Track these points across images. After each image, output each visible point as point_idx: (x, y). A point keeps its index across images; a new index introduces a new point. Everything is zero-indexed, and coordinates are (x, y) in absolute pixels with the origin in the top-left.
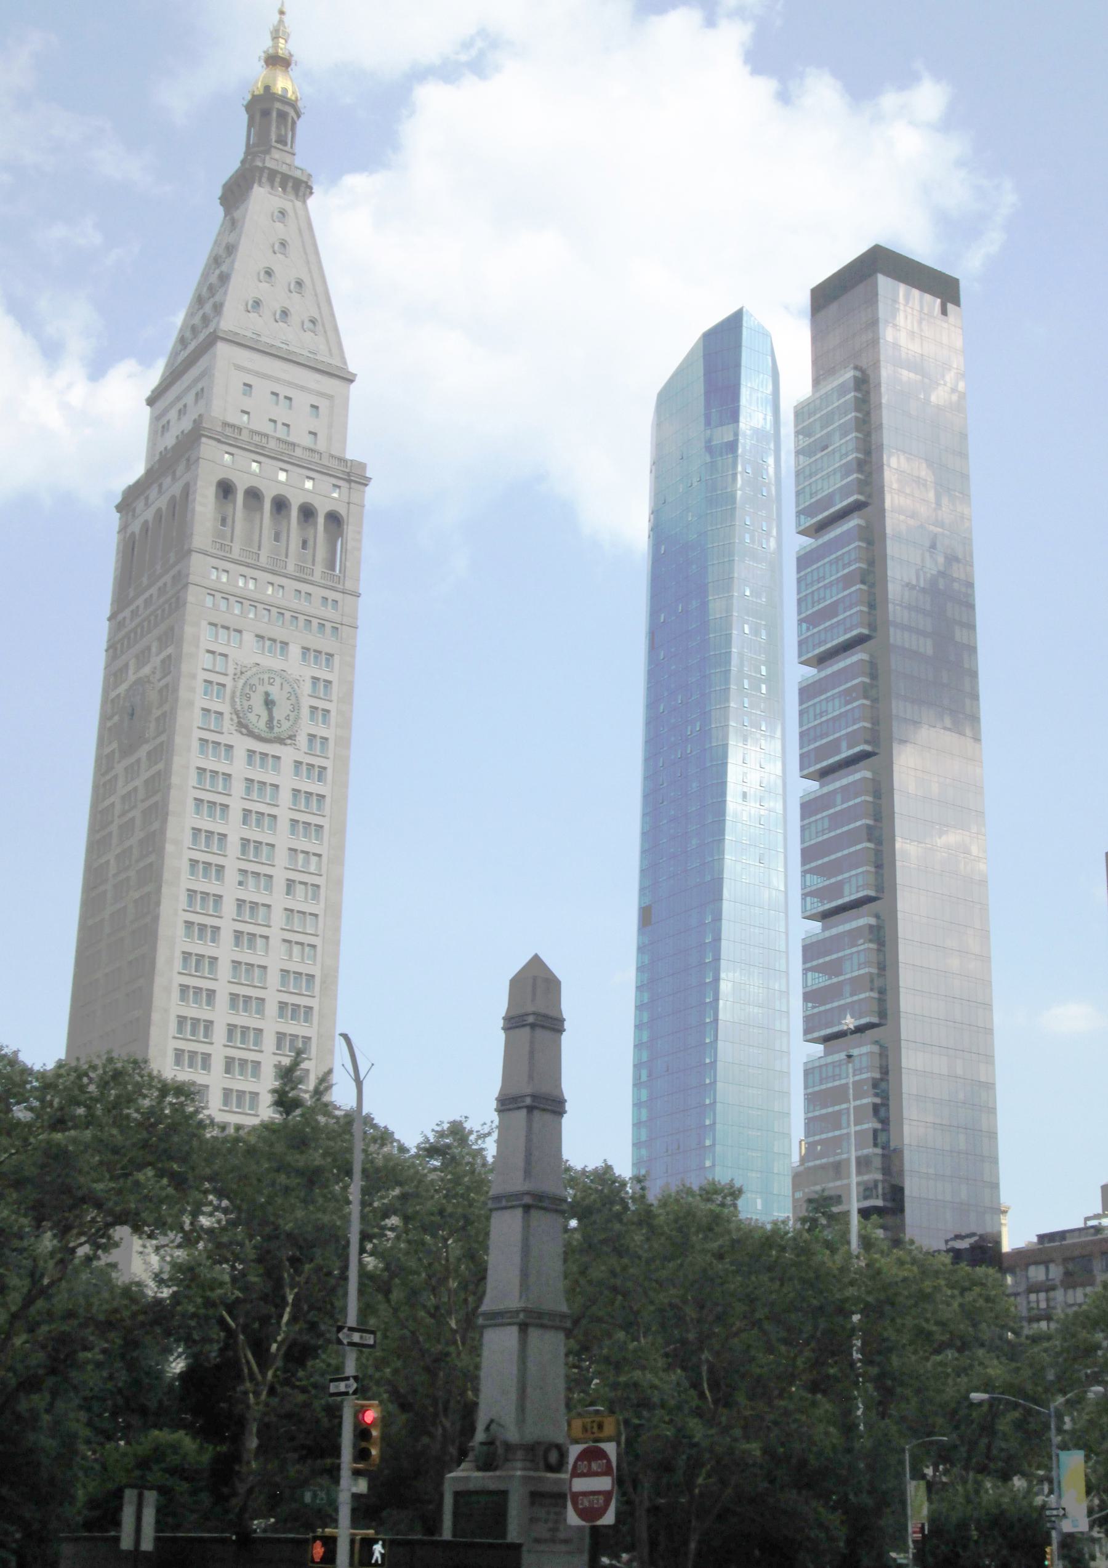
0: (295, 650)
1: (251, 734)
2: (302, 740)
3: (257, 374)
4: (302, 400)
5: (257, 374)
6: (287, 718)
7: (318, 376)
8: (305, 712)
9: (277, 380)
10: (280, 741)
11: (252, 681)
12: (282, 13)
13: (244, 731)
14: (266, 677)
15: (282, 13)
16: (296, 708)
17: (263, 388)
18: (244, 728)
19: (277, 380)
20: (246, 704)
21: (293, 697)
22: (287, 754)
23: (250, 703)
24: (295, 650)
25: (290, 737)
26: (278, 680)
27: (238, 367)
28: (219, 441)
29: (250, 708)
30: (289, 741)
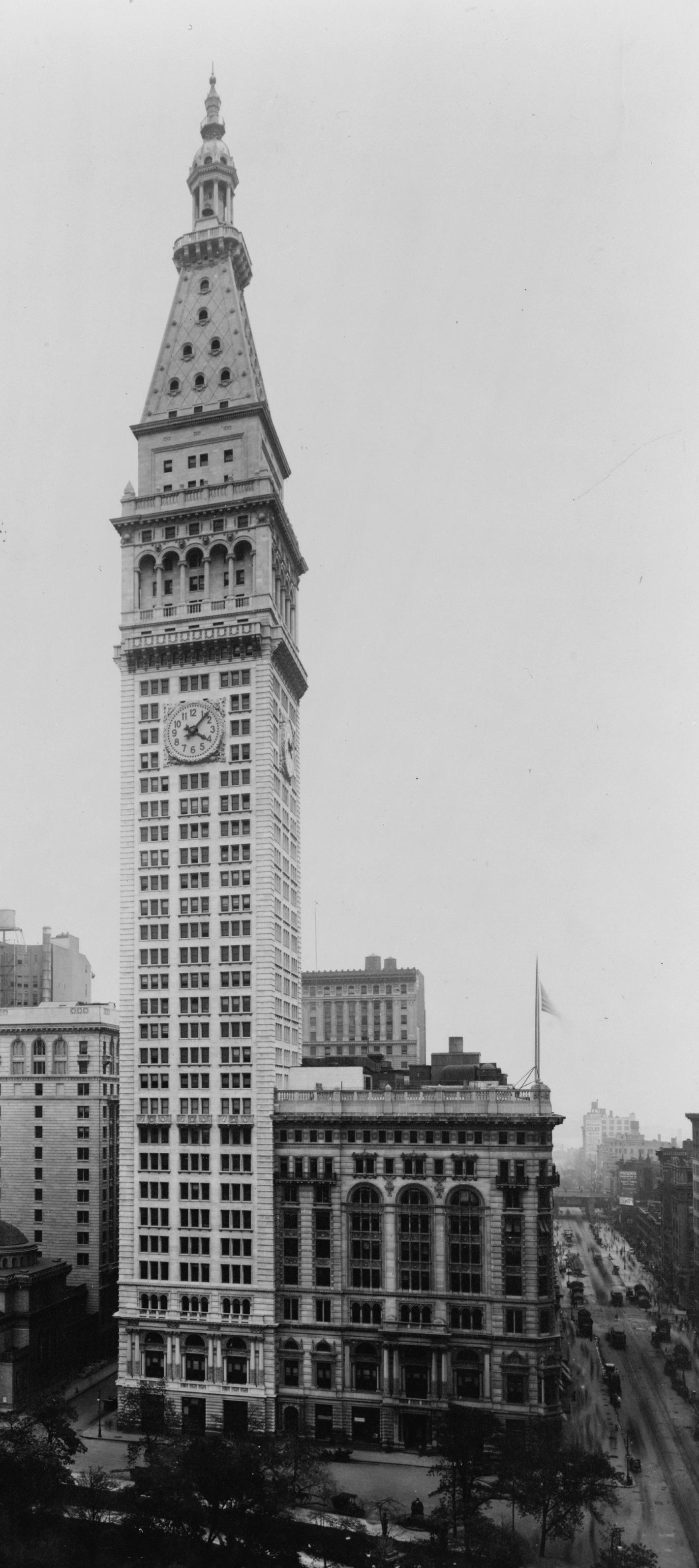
0: (214, 681)
1: (179, 763)
4: (216, 453)
10: (207, 760)
13: (175, 761)
22: (214, 770)
24: (214, 681)
25: (212, 755)
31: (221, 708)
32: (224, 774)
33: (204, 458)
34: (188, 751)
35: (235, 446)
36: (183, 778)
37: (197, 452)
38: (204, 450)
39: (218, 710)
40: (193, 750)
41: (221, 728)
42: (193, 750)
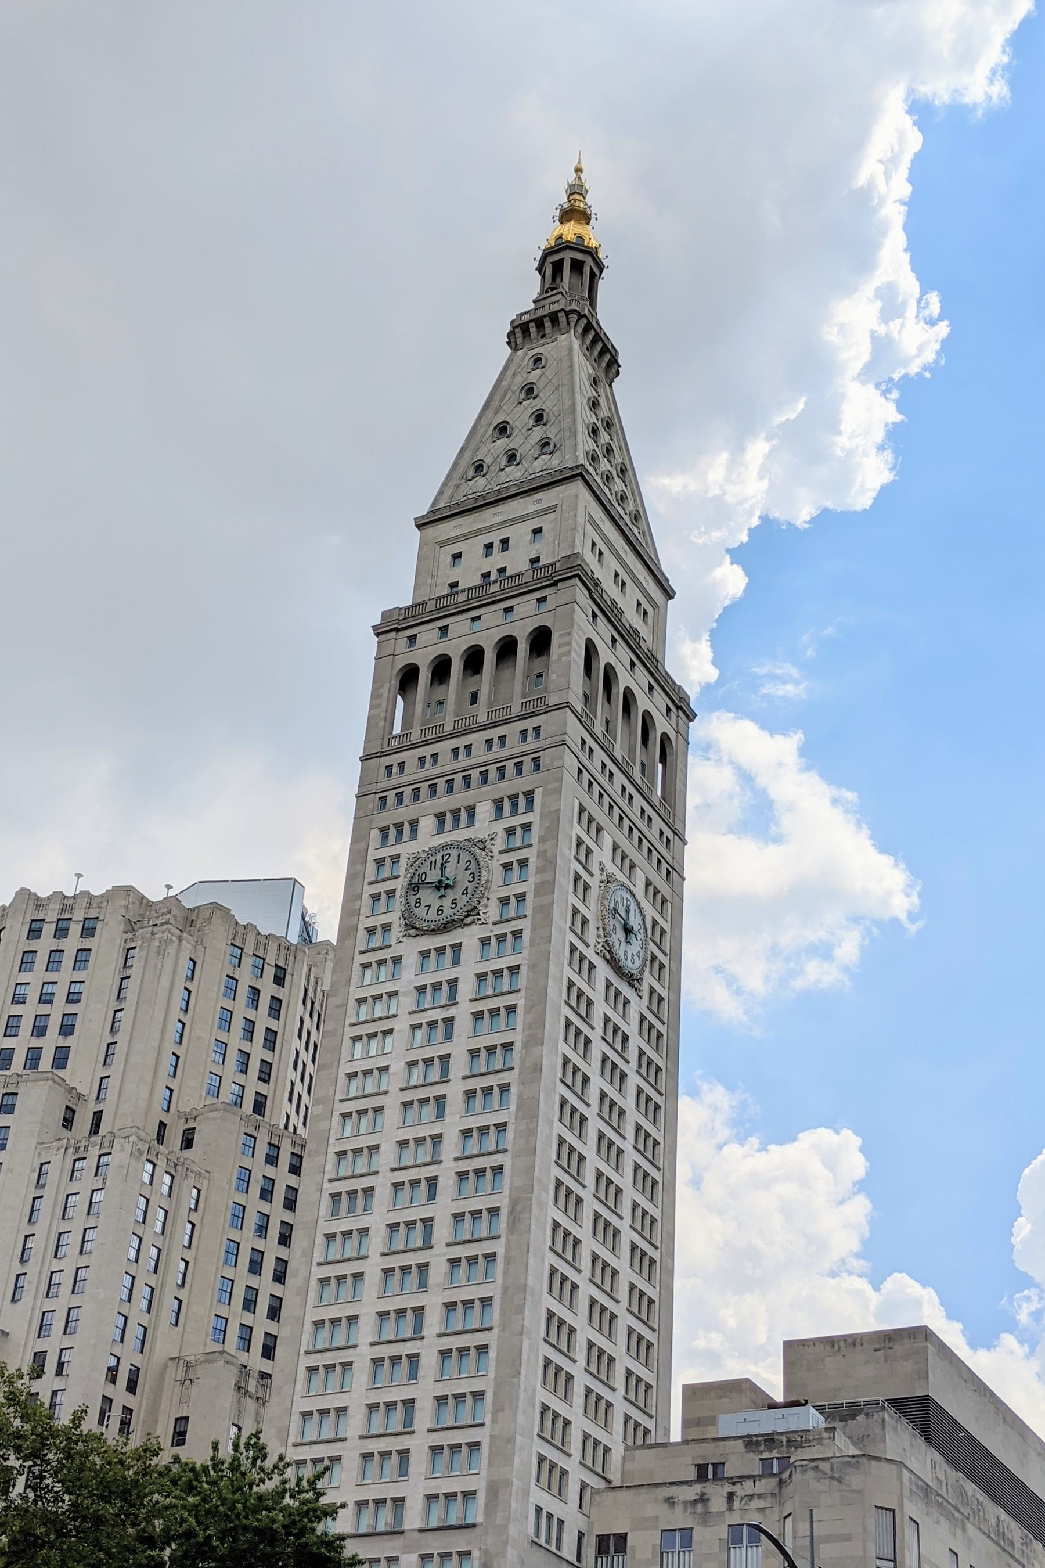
0: (485, 810)
1: (422, 933)
3: (465, 537)
5: (465, 537)
7: (539, 496)
9: (490, 529)
11: (420, 871)
12: (578, 170)
13: (413, 932)
15: (578, 170)
17: (472, 550)
18: (413, 928)
19: (490, 529)
20: (412, 899)
21: (473, 865)
22: (469, 937)
23: (417, 897)
24: (485, 810)
27: (443, 544)
28: (397, 630)
29: (418, 902)
30: (469, 920)
31: (488, 844)
32: (485, 942)
33: (505, 542)
34: (432, 915)
35: (546, 522)
36: (425, 954)
37: (495, 538)
38: (504, 534)
39: (483, 849)
40: (440, 911)
41: (484, 873)
42: (440, 911)
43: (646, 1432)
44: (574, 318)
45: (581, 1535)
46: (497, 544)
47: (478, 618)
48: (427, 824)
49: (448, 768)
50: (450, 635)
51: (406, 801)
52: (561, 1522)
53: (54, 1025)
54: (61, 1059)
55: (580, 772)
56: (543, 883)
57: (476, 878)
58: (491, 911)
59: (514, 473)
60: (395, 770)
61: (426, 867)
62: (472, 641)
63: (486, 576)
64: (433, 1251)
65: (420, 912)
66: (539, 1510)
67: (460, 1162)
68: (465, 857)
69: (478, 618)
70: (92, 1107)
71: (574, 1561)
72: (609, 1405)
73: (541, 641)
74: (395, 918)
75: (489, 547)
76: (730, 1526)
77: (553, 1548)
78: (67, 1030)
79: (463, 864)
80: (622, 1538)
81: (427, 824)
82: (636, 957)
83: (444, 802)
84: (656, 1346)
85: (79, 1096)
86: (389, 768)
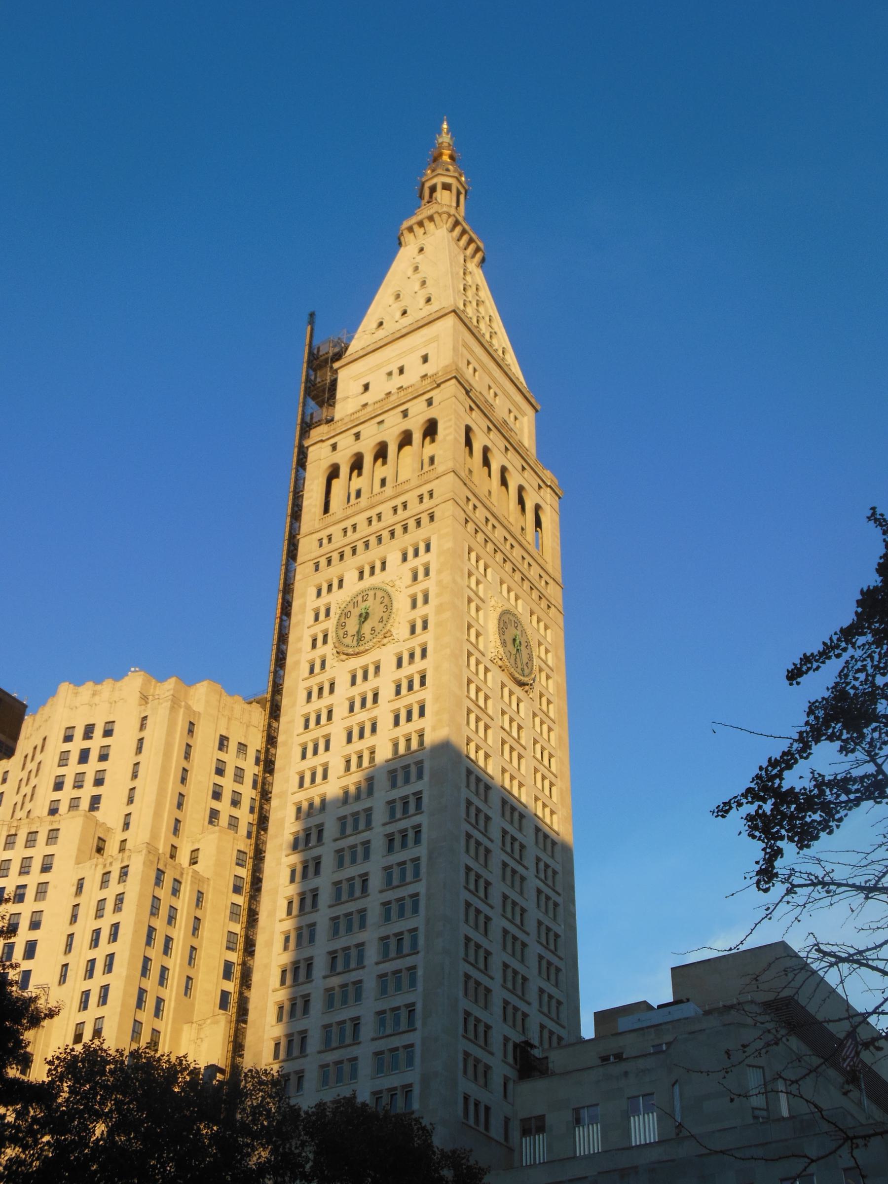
0: (394, 558)
2: (400, 630)
6: (381, 621)
8: (401, 603)
11: (346, 611)
14: (360, 598)
16: (388, 608)
18: (343, 654)
20: (341, 633)
21: (386, 600)
22: (386, 655)
24: (394, 558)
26: (371, 593)
28: (322, 441)
29: (346, 633)
30: (385, 641)
43: (560, 1039)
44: (445, 216)
45: (507, 1120)
46: (396, 372)
47: (382, 422)
48: (350, 577)
49: (364, 534)
50: (362, 438)
51: (333, 563)
52: (487, 1109)
53: (89, 779)
54: (95, 801)
55: (467, 521)
56: (441, 604)
57: (389, 608)
58: (400, 630)
59: (406, 321)
60: (325, 541)
61: (350, 608)
62: (379, 439)
63: (389, 394)
64: (369, 898)
65: (348, 641)
66: (466, 1099)
67: (388, 826)
68: (380, 594)
69: (382, 422)
70: (119, 836)
71: (502, 1141)
72: (525, 1016)
73: (431, 430)
74: (327, 650)
75: (390, 374)
76: (628, 1098)
77: (482, 1128)
78: (99, 782)
79: (378, 600)
80: (541, 1118)
81: (350, 577)
82: (525, 668)
83: (363, 558)
84: (564, 971)
85: (109, 830)
86: (321, 540)
